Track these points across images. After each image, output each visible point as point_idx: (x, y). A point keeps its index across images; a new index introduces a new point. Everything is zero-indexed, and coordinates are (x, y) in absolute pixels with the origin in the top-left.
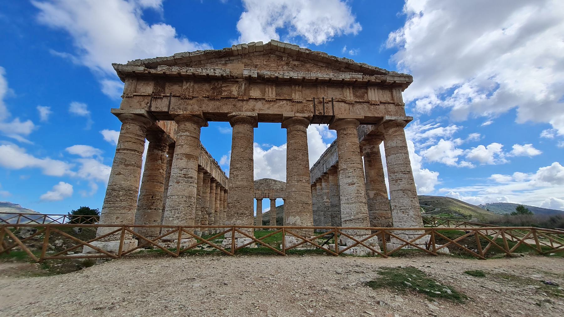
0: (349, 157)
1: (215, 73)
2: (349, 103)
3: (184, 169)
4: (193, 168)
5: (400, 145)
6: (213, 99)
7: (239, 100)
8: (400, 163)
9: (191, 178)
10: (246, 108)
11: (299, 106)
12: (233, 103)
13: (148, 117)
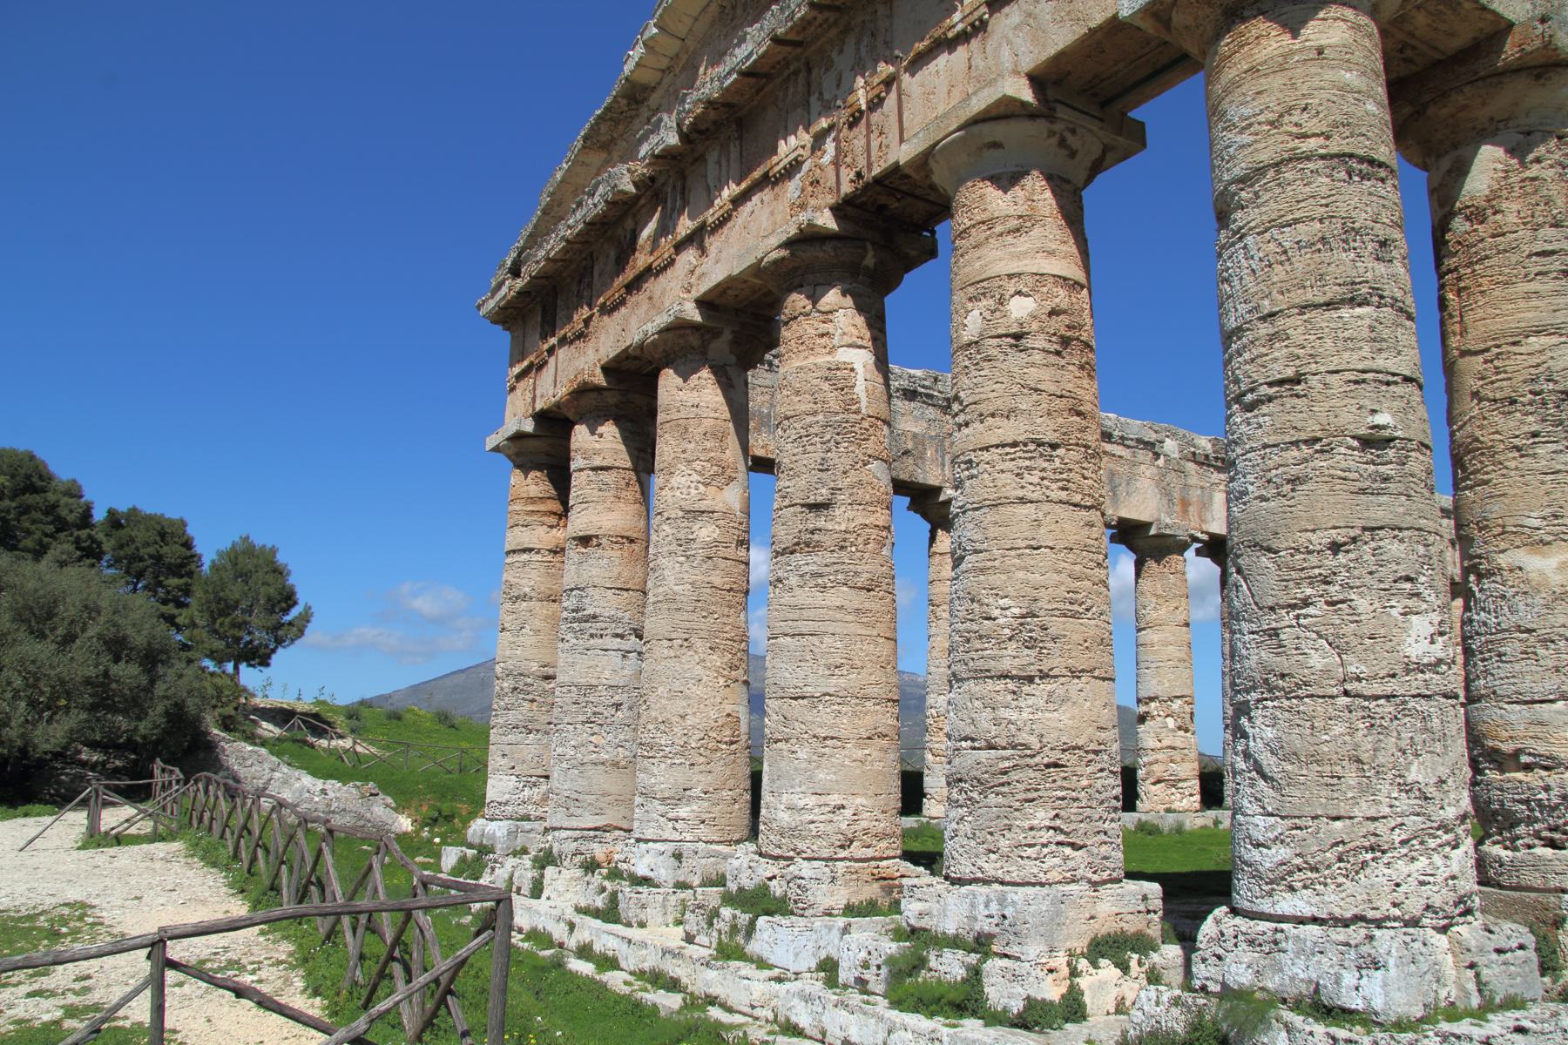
1: (595, 205)
2: (964, 32)
4: (596, 581)
5: (1237, 172)
9: (595, 617)
11: (792, 188)
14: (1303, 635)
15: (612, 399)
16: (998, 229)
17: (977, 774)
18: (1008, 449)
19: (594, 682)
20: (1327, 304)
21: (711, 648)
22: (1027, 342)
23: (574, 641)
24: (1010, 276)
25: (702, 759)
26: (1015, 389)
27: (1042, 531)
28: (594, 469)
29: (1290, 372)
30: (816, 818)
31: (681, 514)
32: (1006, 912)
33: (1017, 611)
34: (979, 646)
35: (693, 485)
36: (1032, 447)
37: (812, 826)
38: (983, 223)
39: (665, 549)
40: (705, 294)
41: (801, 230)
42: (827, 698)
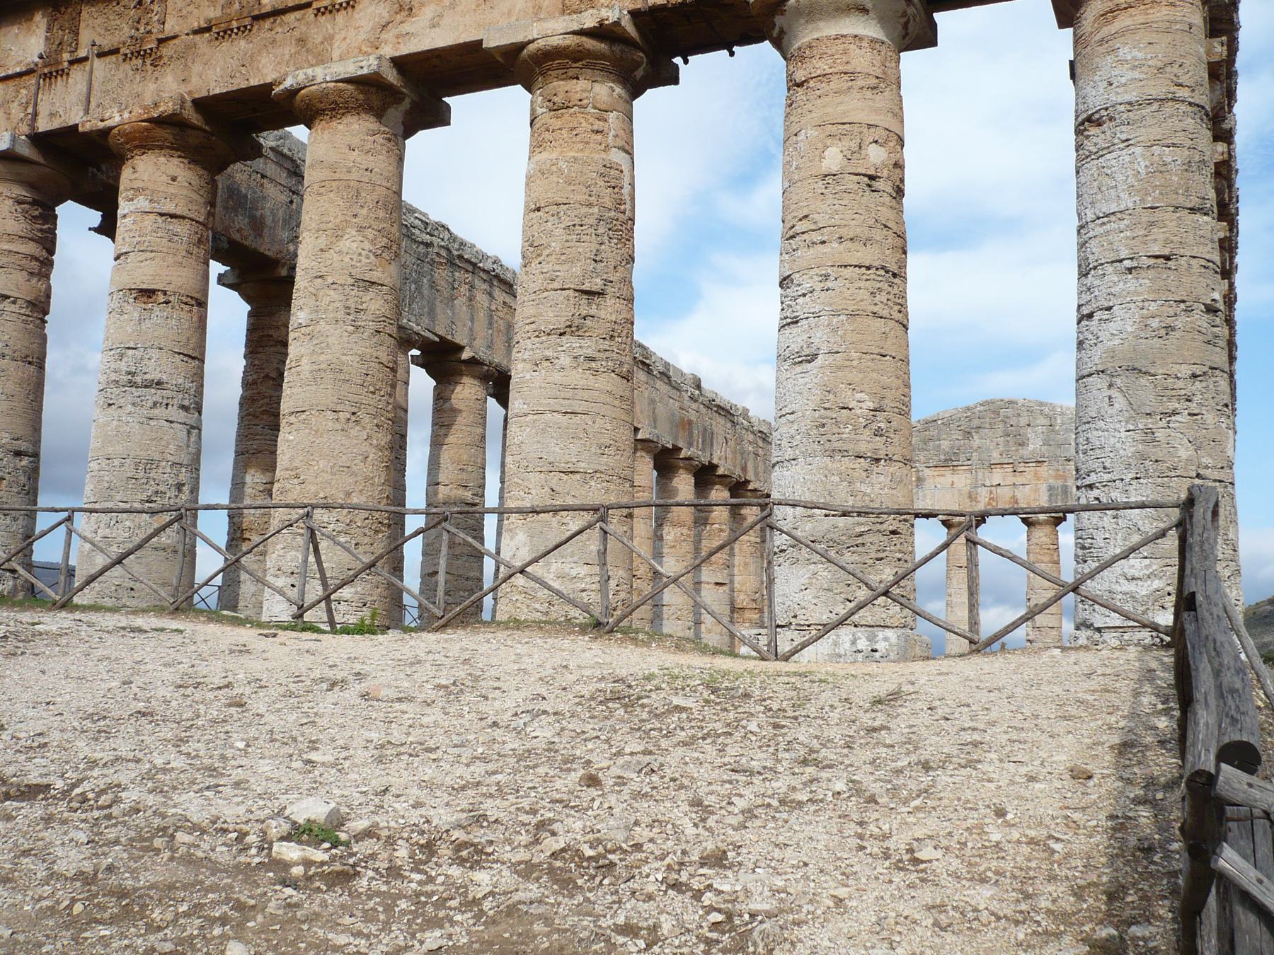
0: (805, 212)
3: (131, 352)
5: (1127, 98)
6: (225, 32)
7: (318, 10)
8: (1114, 208)
9: (159, 383)
10: (344, 46)
12: (296, 33)
13: (41, 160)
14: (1173, 434)
15: (193, 139)
16: (860, 83)
17: (835, 536)
18: (863, 270)
19: (157, 456)
20: (1190, 209)
21: (377, 426)
22: (877, 185)
23: (130, 408)
24: (869, 126)
25: (366, 540)
26: (872, 222)
27: (889, 342)
28: (162, 215)
29: (1166, 252)
30: (588, 587)
31: (351, 281)
32: (877, 646)
33: (871, 405)
34: (836, 430)
35: (364, 253)
36: (882, 272)
37: (584, 594)
38: (845, 73)
39: (332, 315)
40: (409, 55)
41: (601, 25)
42: (598, 475)
